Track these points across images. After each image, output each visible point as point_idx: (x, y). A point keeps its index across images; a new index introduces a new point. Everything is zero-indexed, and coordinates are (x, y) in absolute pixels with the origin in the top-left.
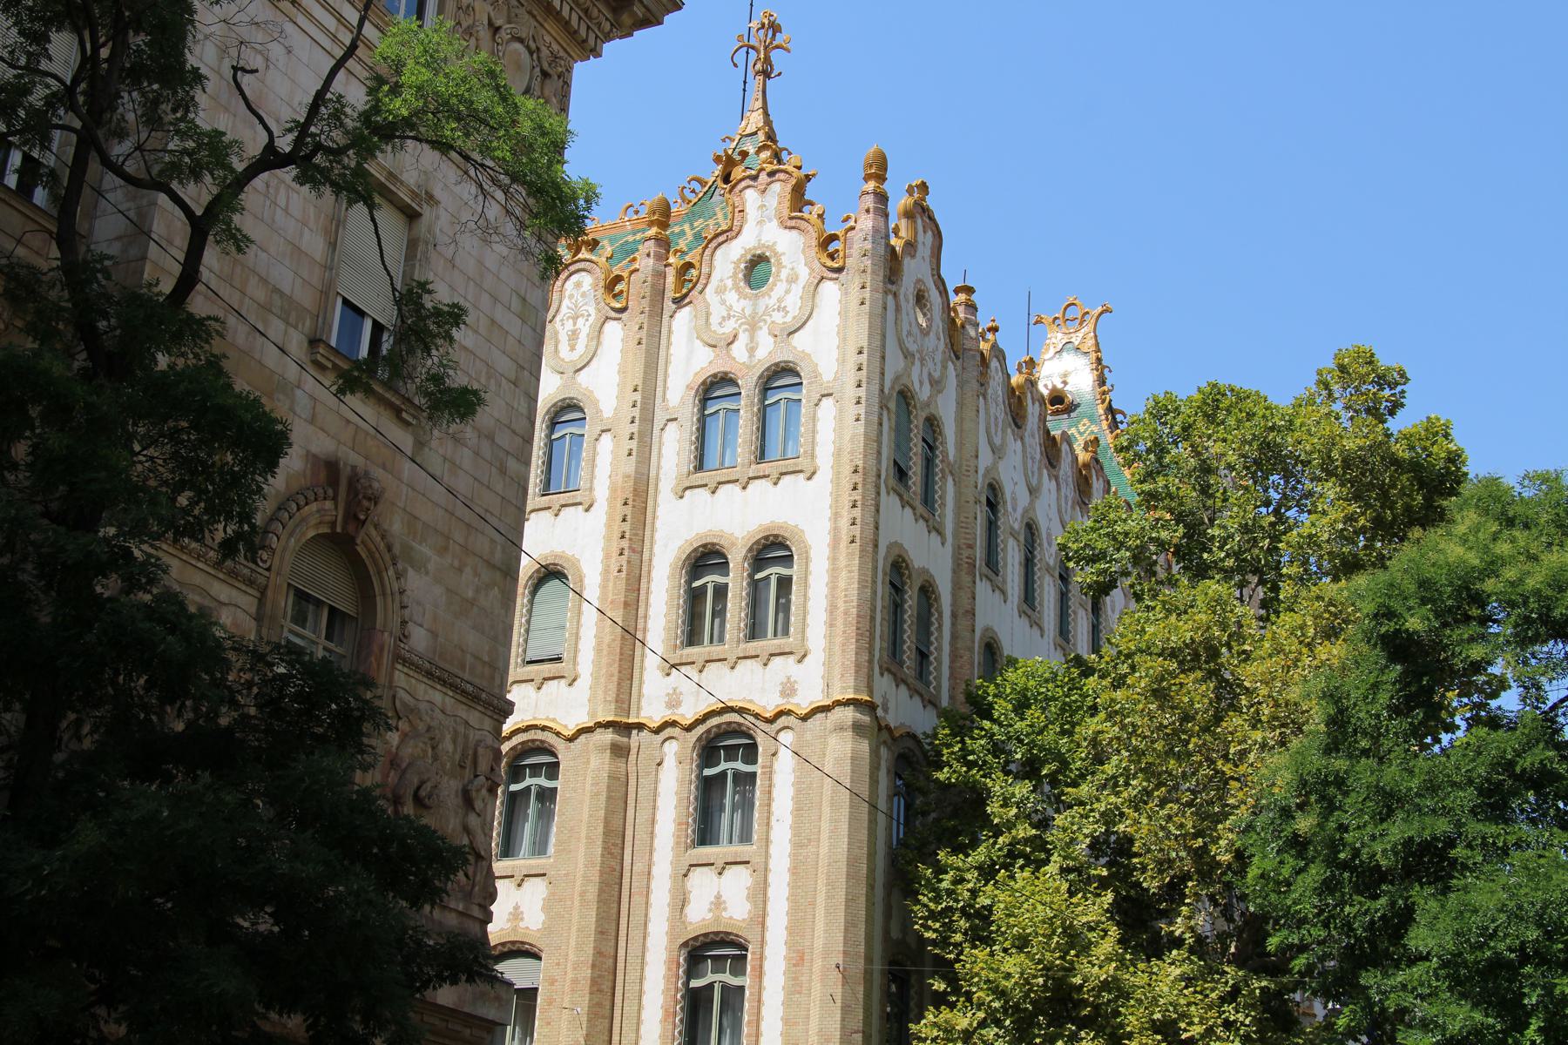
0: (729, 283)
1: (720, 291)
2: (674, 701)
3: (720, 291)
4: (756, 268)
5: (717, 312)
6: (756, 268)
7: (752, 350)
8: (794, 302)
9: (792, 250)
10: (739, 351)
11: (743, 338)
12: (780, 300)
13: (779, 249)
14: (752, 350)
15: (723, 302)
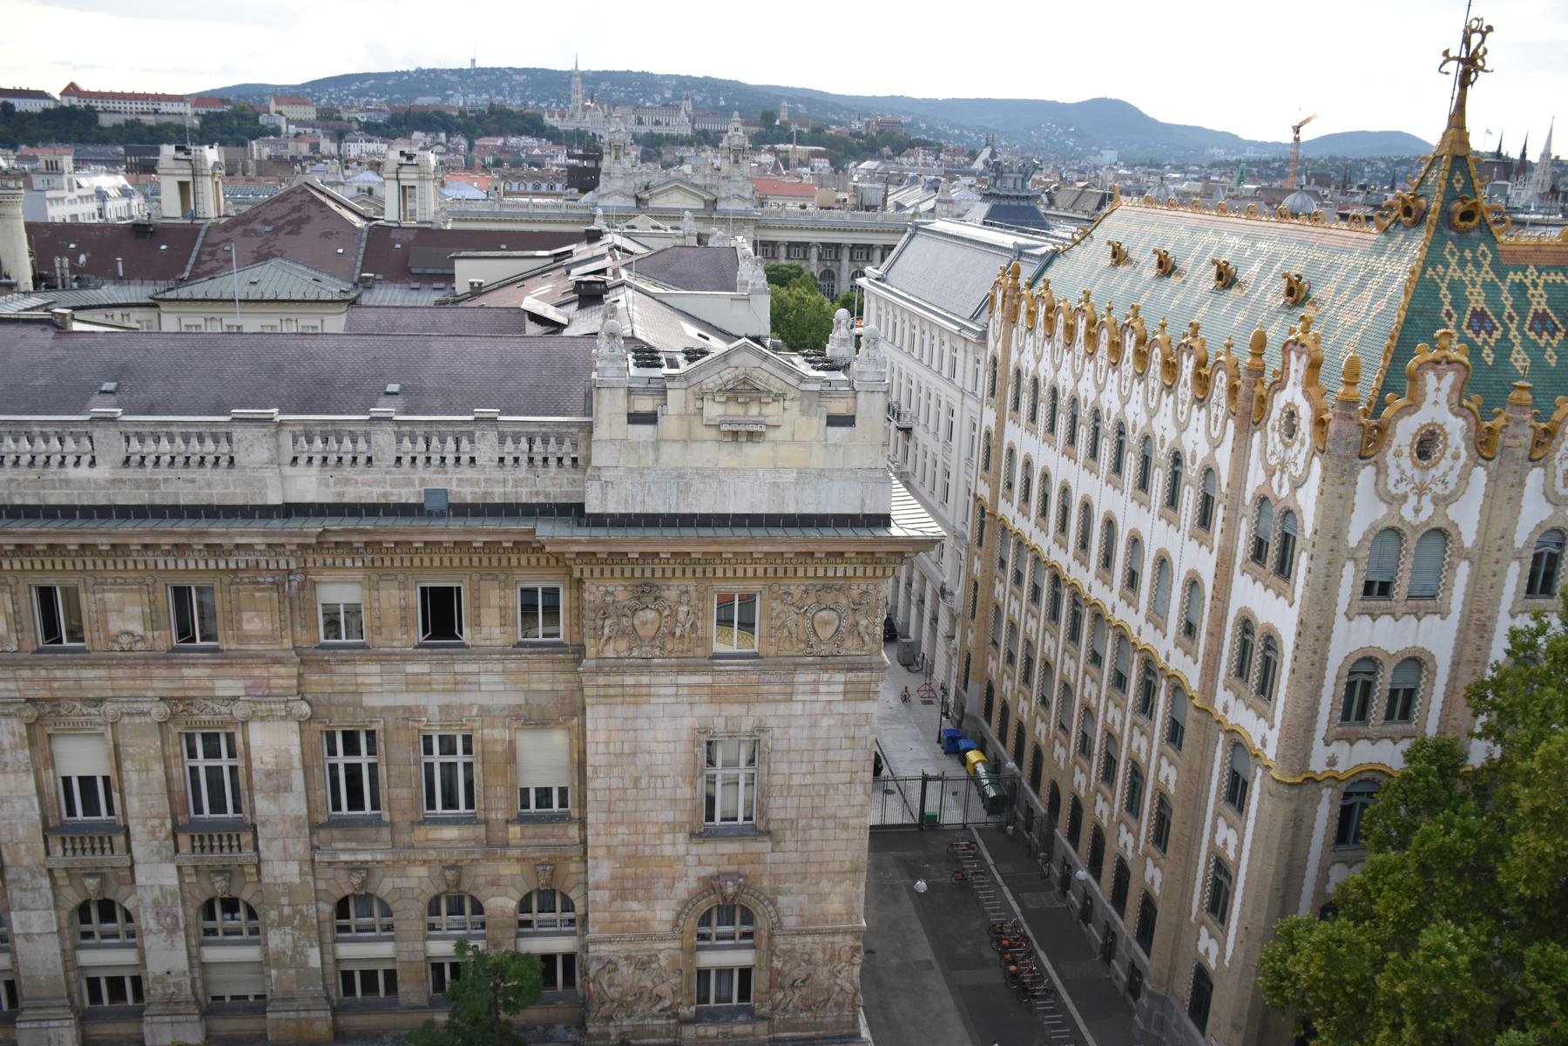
0: (1406, 451)
1: (1398, 454)
2: (1332, 762)
3: (1398, 454)
4: (1426, 446)
5: (1394, 474)
6: (1426, 446)
7: (1417, 511)
8: (1452, 479)
9: (1456, 429)
10: (1407, 512)
11: (1413, 500)
12: (1445, 474)
13: (1447, 429)
14: (1417, 511)
15: (1398, 466)
